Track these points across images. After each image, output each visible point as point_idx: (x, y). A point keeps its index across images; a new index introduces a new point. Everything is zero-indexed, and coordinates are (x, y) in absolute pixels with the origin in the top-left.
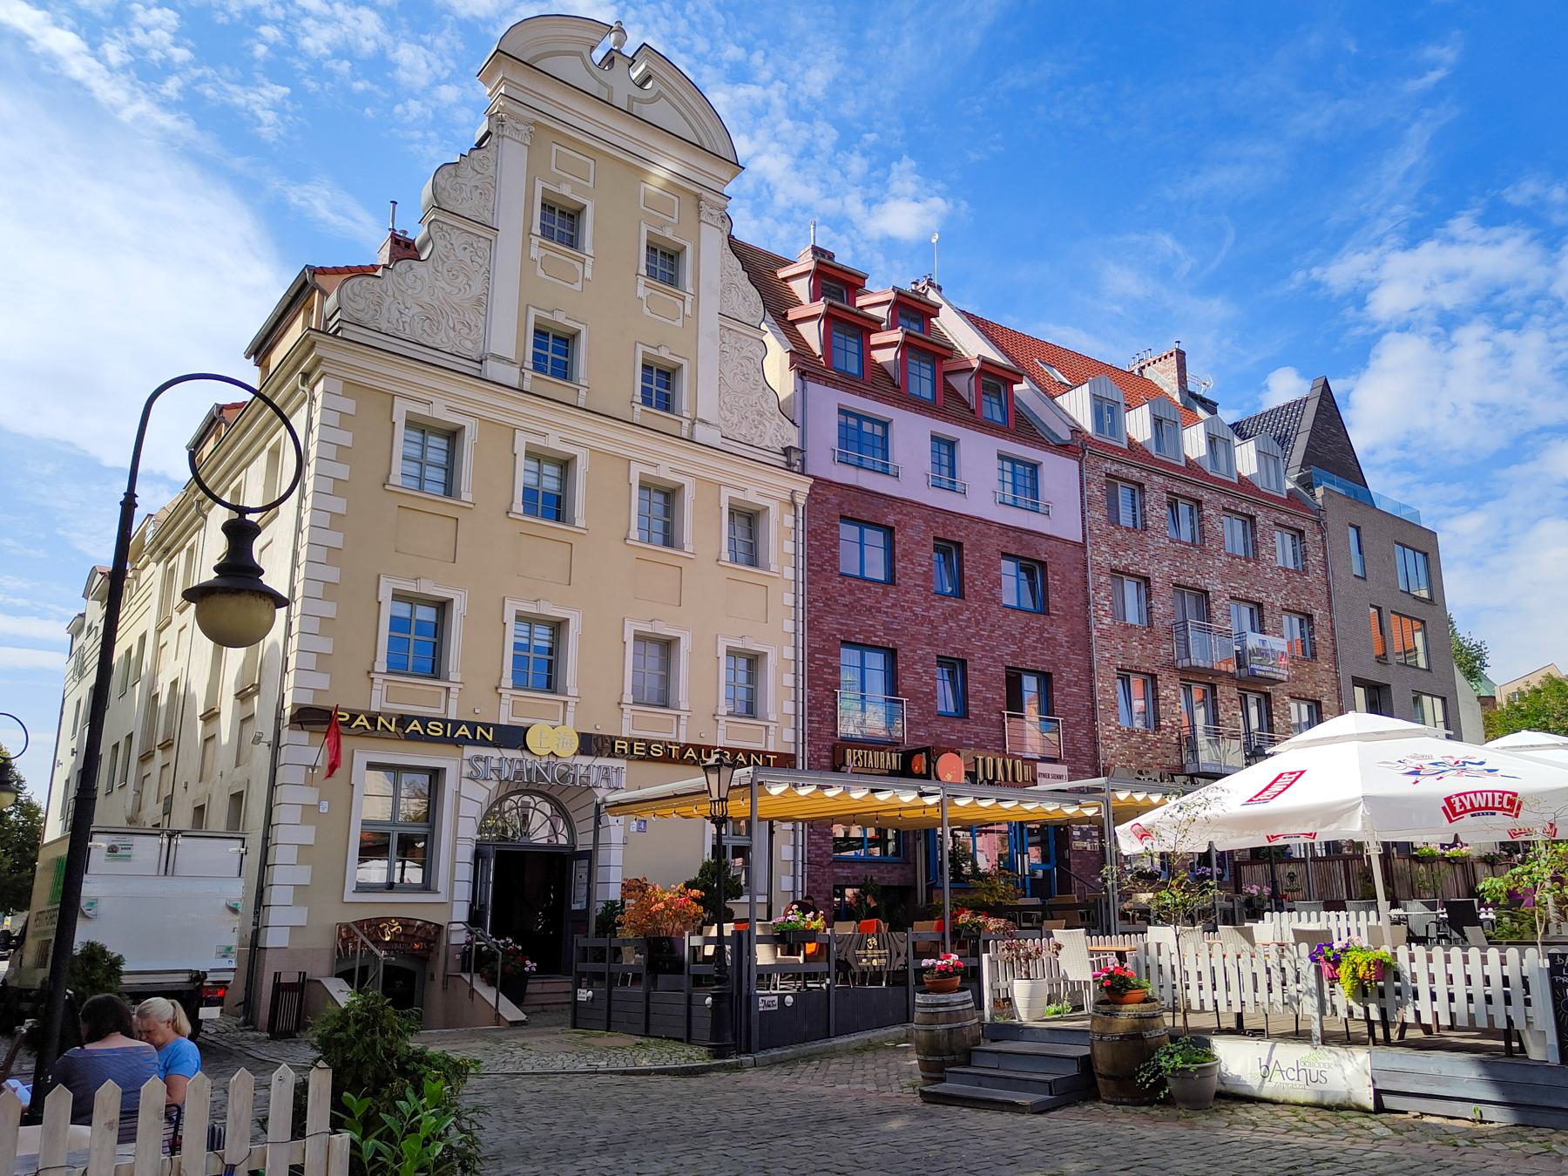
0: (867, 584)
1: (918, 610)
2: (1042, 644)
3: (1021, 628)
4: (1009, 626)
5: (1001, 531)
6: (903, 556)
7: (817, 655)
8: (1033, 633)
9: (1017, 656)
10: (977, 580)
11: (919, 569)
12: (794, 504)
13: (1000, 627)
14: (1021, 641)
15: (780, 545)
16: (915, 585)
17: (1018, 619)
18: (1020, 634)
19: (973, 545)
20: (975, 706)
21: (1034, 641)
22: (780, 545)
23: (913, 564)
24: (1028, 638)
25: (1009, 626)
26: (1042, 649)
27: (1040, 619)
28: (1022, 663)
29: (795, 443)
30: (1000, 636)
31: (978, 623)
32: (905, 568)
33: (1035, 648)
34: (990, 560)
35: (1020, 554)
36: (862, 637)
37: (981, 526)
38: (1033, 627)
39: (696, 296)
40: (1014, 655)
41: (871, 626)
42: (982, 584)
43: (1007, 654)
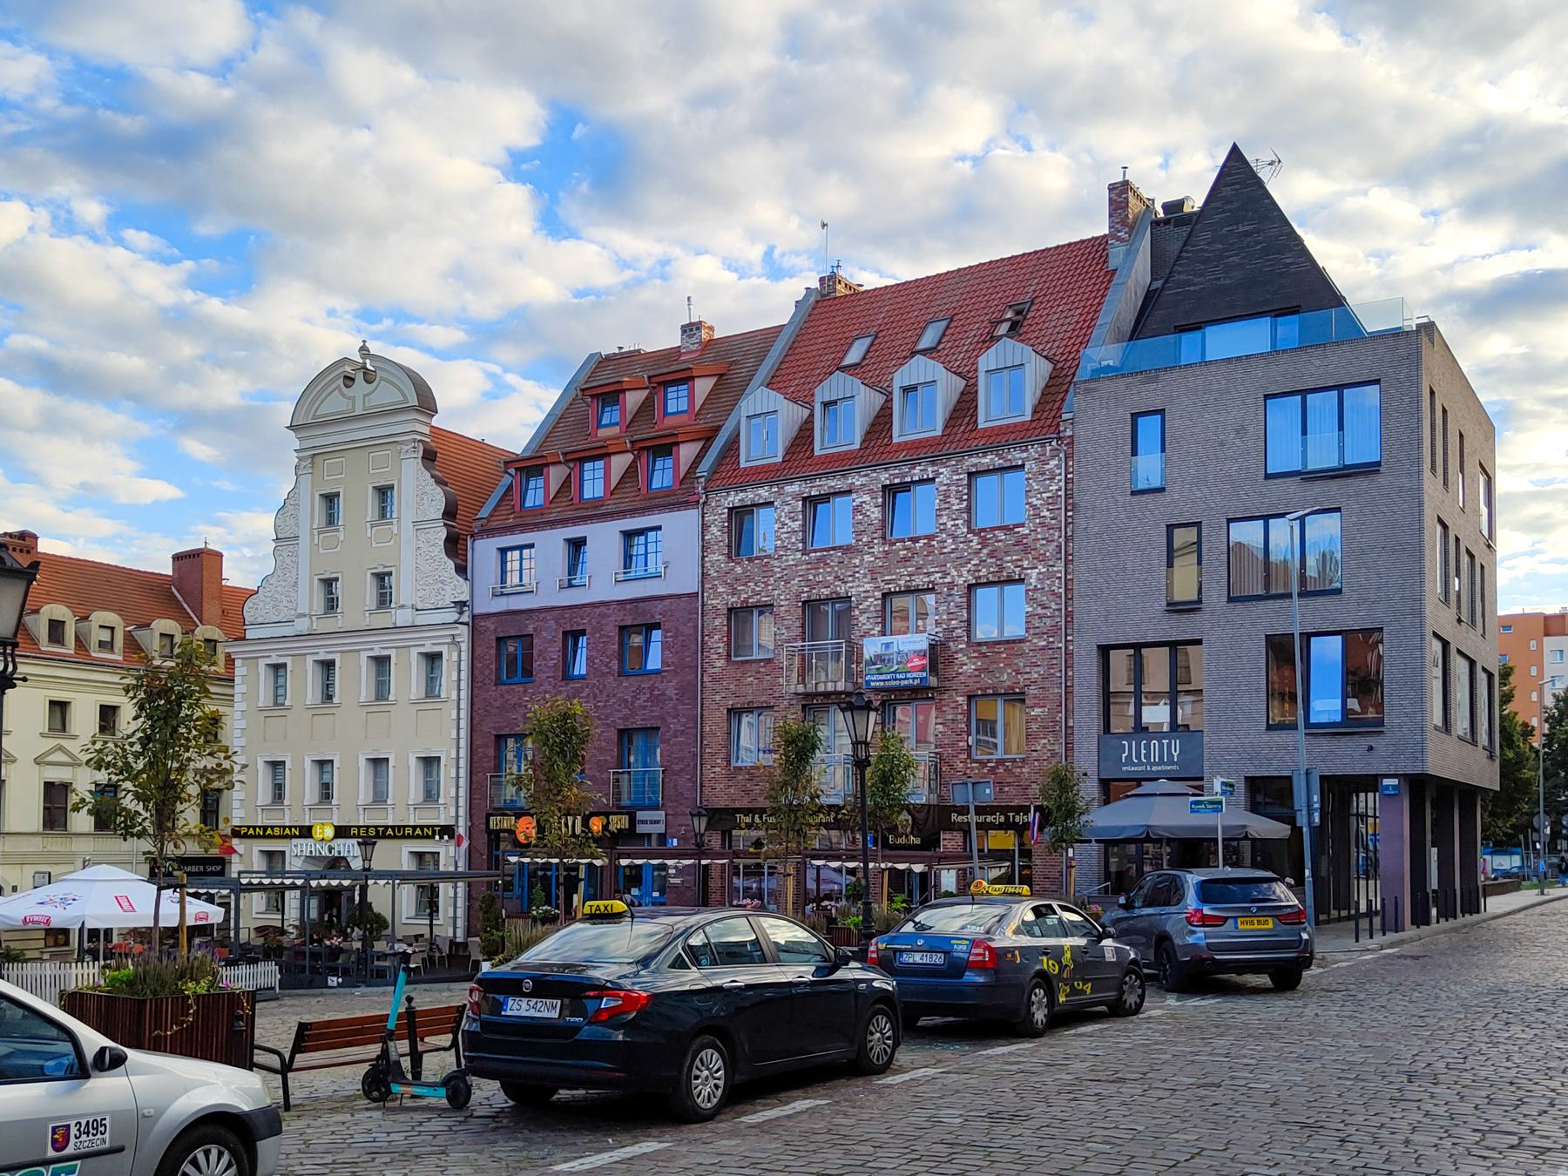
0: (513, 687)
2: (652, 701)
3: (633, 692)
4: (623, 692)
5: (618, 607)
6: (539, 656)
8: (645, 694)
9: (628, 719)
10: (596, 658)
11: (551, 663)
13: (614, 696)
14: (633, 703)
15: (449, 674)
16: (548, 677)
17: (630, 684)
18: (632, 697)
19: (593, 628)
20: (590, 769)
21: (645, 701)
22: (449, 674)
23: (545, 659)
25: (623, 692)
26: (651, 706)
27: (651, 680)
28: (632, 723)
30: (614, 703)
31: (595, 697)
32: (540, 665)
33: (645, 708)
34: (609, 637)
37: (603, 609)
40: (625, 718)
43: (619, 718)
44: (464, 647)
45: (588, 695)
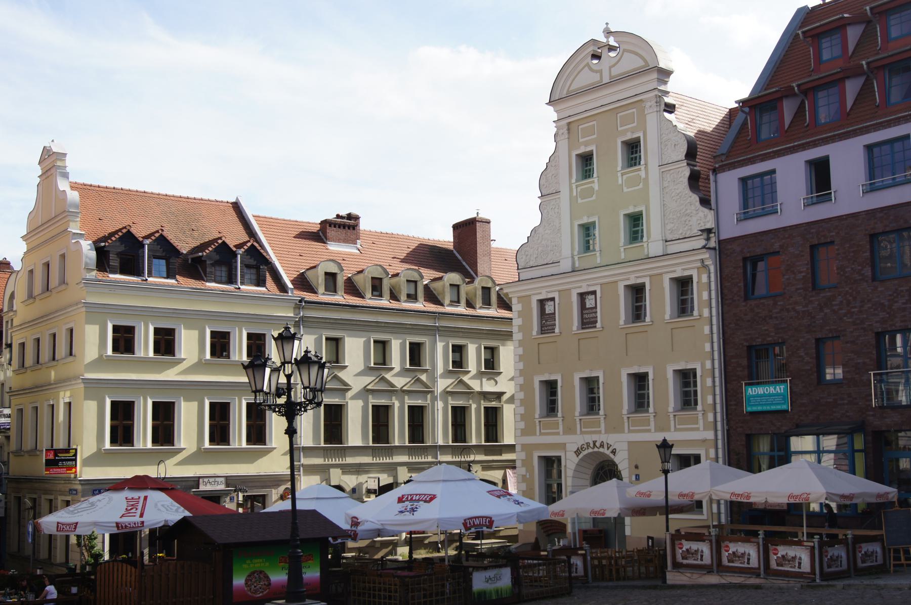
0: (762, 301)
1: (799, 308)
3: (890, 295)
7: (733, 360)
11: (800, 276)
12: (705, 266)
16: (797, 289)
21: (904, 303)
24: (897, 302)
29: (710, 225)
35: (888, 229)
36: (760, 340)
38: (902, 291)
39: (646, 164)
41: (766, 330)
42: (852, 269)
43: (877, 322)
44: (712, 269)
45: (841, 302)
